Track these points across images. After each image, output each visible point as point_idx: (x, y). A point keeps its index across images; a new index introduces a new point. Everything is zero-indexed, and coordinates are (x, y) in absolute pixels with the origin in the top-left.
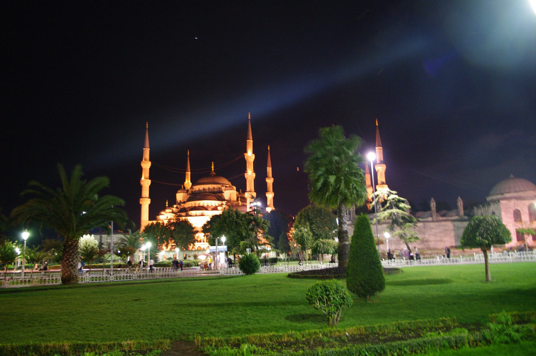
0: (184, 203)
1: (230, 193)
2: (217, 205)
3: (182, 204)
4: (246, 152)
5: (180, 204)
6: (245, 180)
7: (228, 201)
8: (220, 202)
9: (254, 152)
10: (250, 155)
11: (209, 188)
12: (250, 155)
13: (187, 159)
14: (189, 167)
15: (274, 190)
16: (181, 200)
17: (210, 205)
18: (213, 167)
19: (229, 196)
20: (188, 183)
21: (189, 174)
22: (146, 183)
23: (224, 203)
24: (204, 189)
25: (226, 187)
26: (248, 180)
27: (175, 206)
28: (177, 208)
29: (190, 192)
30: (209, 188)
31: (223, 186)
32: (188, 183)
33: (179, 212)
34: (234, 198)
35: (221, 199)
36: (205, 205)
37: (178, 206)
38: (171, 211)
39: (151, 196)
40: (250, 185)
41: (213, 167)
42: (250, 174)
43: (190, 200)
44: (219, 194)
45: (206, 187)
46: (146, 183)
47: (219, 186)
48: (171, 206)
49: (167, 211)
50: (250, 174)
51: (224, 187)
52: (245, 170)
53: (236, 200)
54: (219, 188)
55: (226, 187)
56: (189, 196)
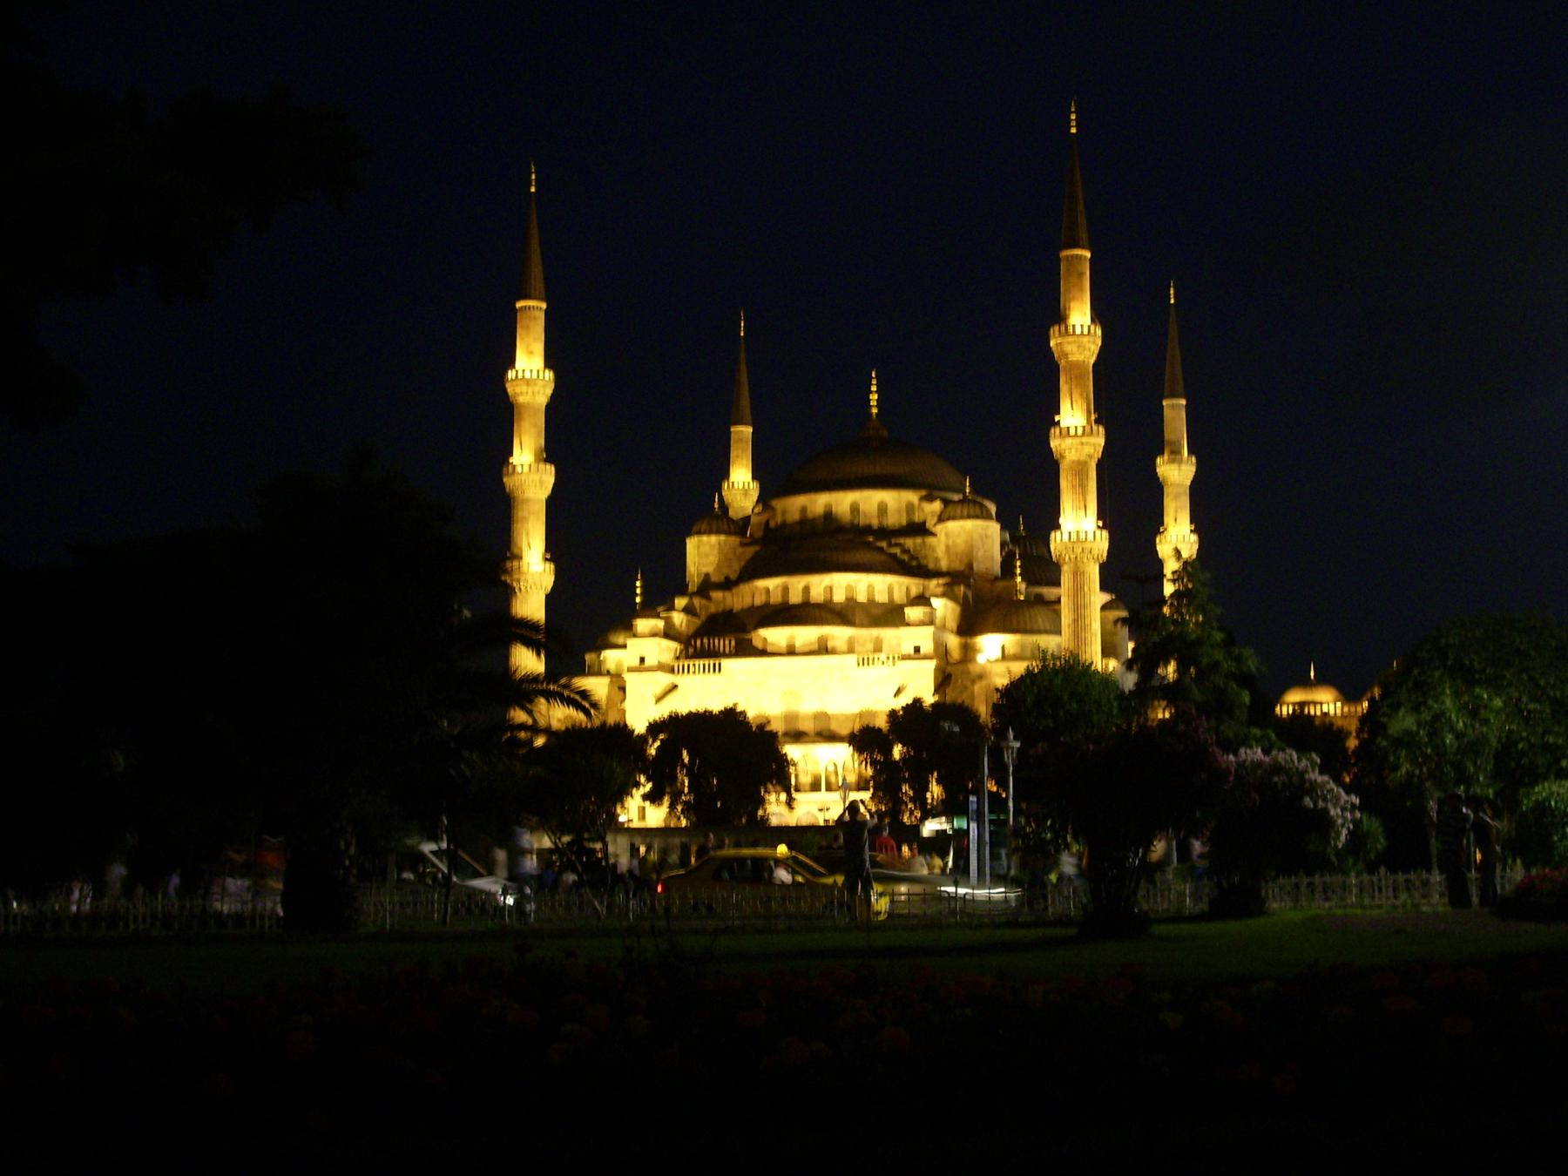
0: (728, 585)
1: (971, 536)
2: (899, 597)
3: (717, 595)
4: (1059, 317)
5: (706, 587)
6: (1049, 467)
8: (913, 585)
9: (1098, 315)
10: (1079, 333)
11: (855, 509)
12: (1079, 333)
14: (745, 401)
16: (710, 569)
17: (862, 598)
20: (741, 478)
21: (743, 433)
22: (530, 473)
23: (934, 584)
24: (829, 516)
25: (946, 502)
26: (1063, 466)
27: (681, 602)
28: (688, 610)
30: (855, 509)
31: (929, 498)
32: (741, 478)
33: (700, 632)
36: (839, 597)
37: (697, 601)
38: (659, 624)
42: (1076, 431)
44: (909, 542)
45: (843, 502)
46: (530, 473)
47: (911, 496)
48: (657, 602)
49: (642, 625)
51: (937, 506)
53: (997, 569)
56: (751, 550)
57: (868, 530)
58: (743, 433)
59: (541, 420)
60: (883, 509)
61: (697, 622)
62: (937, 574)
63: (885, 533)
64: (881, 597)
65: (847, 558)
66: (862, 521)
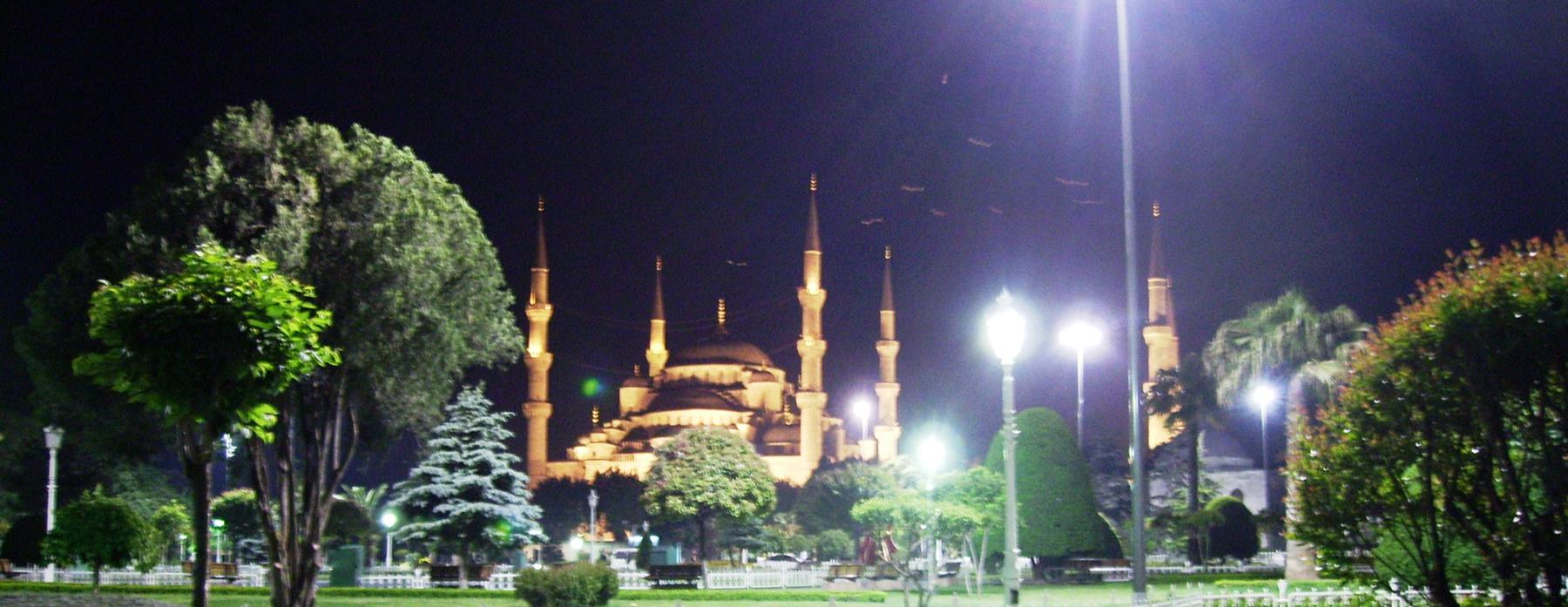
0: (641, 413)
3: (635, 419)
4: (802, 284)
5: (630, 414)
7: (759, 412)
10: (813, 293)
12: (813, 293)
13: (653, 288)
15: (900, 377)
18: (721, 314)
19: (759, 397)
20: (657, 351)
23: (746, 415)
24: (694, 378)
25: (755, 372)
26: (804, 359)
27: (616, 423)
28: (620, 428)
29: (657, 386)
32: (657, 351)
33: (626, 439)
34: (775, 403)
35: (737, 406)
37: (625, 423)
38: (602, 436)
39: (551, 399)
40: (811, 372)
41: (721, 314)
43: (654, 406)
44: (734, 393)
47: (736, 368)
49: (595, 436)
50: (811, 346)
52: (797, 334)
53: (778, 408)
54: (736, 375)
55: (755, 372)
57: (713, 386)
58: (658, 325)
59: (544, 330)
60: (721, 375)
61: (624, 433)
62: (747, 409)
63: (722, 387)
64: (717, 422)
65: (703, 401)
66: (711, 380)
